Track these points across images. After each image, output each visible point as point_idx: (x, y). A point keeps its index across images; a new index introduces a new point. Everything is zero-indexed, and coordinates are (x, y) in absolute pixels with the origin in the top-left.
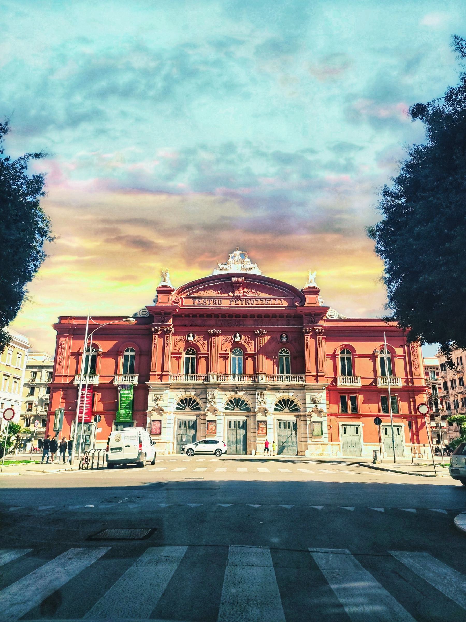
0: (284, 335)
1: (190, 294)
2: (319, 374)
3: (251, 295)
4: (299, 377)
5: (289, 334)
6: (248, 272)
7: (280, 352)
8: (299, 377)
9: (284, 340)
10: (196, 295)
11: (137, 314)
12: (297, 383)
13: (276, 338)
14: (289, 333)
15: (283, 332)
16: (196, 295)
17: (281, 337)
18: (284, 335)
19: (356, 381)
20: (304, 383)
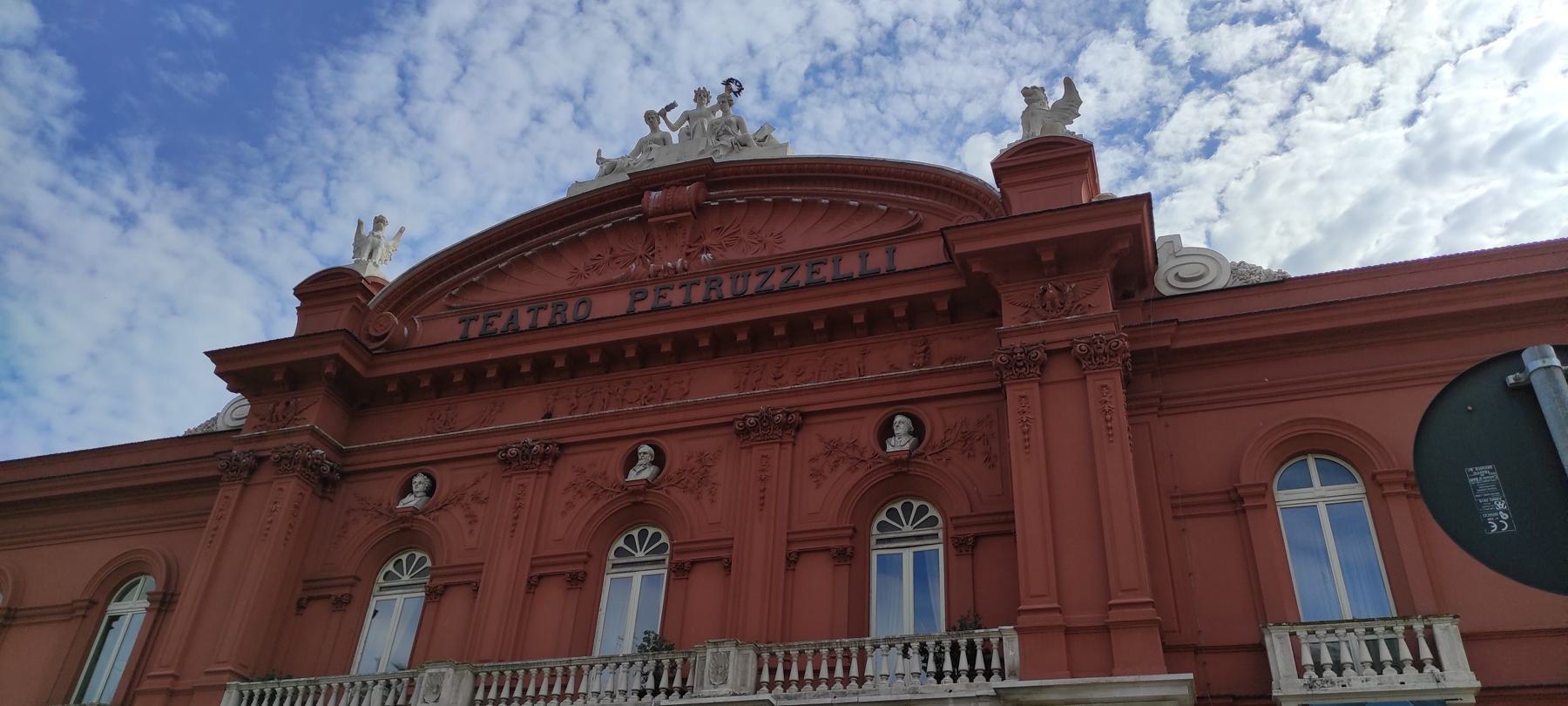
0: (902, 424)
1: (452, 296)
2: (1116, 616)
3: (732, 255)
4: (971, 648)
5: (927, 413)
6: (722, 157)
7: (883, 527)
8: (971, 648)
9: (900, 442)
10: (484, 297)
11: (215, 419)
12: (962, 687)
13: (854, 445)
14: (931, 408)
15: (898, 406)
16: (484, 297)
17: (887, 431)
18: (902, 424)
19: (1426, 653)
20: (1011, 683)
